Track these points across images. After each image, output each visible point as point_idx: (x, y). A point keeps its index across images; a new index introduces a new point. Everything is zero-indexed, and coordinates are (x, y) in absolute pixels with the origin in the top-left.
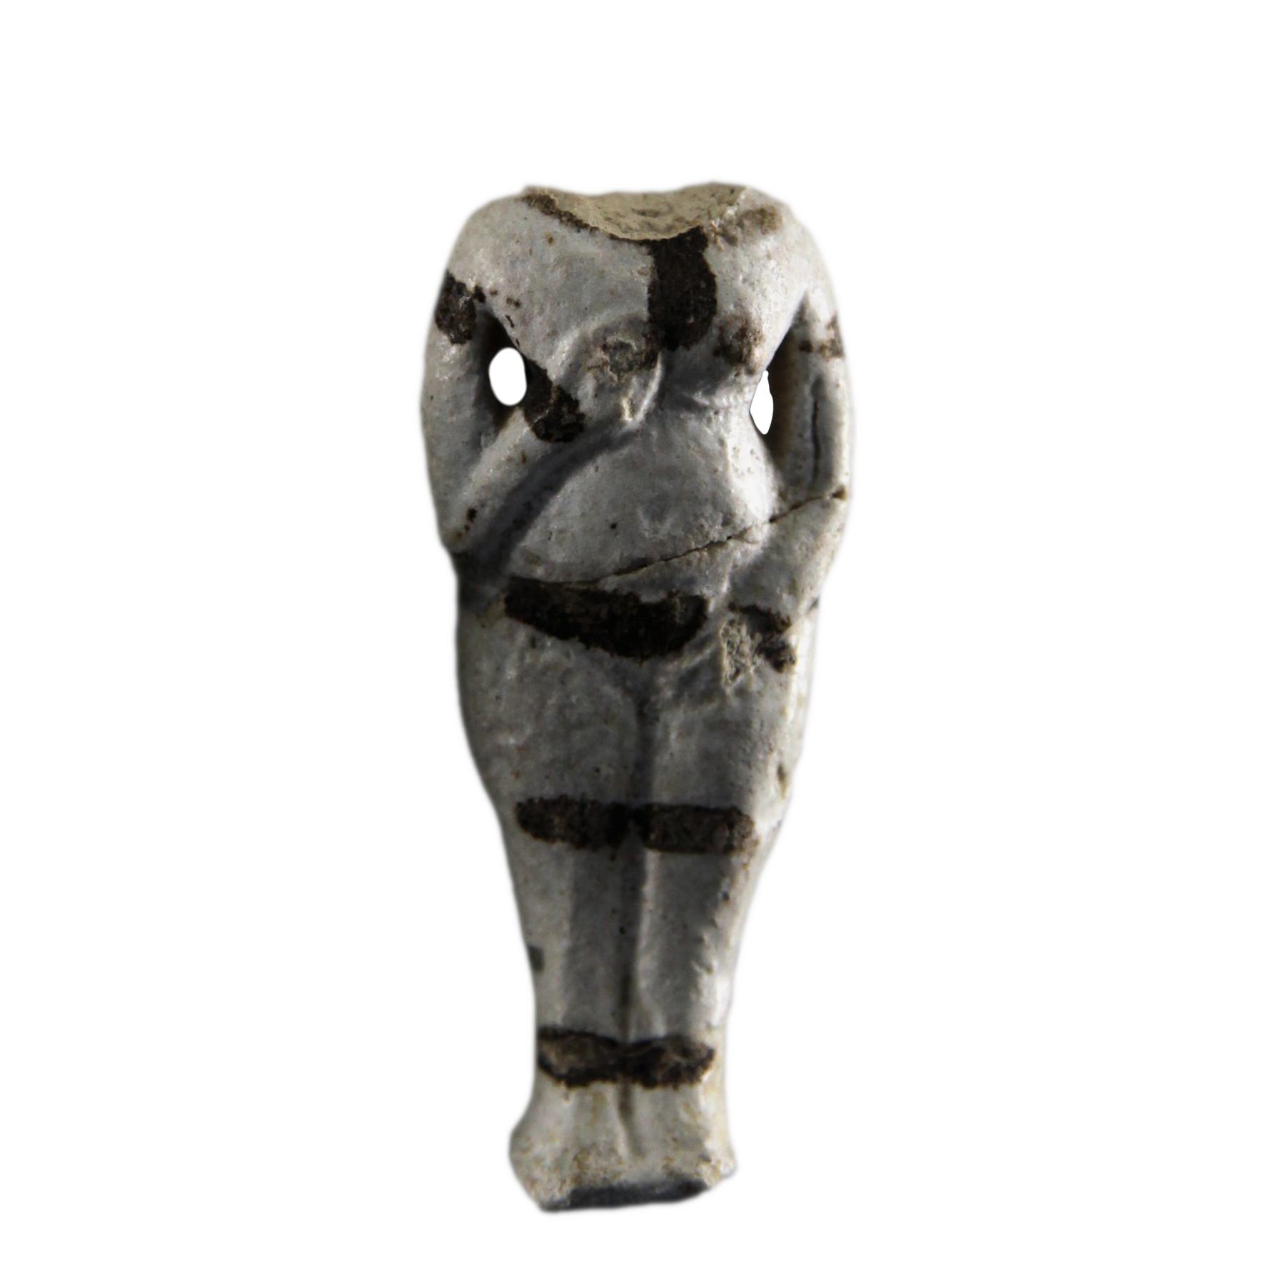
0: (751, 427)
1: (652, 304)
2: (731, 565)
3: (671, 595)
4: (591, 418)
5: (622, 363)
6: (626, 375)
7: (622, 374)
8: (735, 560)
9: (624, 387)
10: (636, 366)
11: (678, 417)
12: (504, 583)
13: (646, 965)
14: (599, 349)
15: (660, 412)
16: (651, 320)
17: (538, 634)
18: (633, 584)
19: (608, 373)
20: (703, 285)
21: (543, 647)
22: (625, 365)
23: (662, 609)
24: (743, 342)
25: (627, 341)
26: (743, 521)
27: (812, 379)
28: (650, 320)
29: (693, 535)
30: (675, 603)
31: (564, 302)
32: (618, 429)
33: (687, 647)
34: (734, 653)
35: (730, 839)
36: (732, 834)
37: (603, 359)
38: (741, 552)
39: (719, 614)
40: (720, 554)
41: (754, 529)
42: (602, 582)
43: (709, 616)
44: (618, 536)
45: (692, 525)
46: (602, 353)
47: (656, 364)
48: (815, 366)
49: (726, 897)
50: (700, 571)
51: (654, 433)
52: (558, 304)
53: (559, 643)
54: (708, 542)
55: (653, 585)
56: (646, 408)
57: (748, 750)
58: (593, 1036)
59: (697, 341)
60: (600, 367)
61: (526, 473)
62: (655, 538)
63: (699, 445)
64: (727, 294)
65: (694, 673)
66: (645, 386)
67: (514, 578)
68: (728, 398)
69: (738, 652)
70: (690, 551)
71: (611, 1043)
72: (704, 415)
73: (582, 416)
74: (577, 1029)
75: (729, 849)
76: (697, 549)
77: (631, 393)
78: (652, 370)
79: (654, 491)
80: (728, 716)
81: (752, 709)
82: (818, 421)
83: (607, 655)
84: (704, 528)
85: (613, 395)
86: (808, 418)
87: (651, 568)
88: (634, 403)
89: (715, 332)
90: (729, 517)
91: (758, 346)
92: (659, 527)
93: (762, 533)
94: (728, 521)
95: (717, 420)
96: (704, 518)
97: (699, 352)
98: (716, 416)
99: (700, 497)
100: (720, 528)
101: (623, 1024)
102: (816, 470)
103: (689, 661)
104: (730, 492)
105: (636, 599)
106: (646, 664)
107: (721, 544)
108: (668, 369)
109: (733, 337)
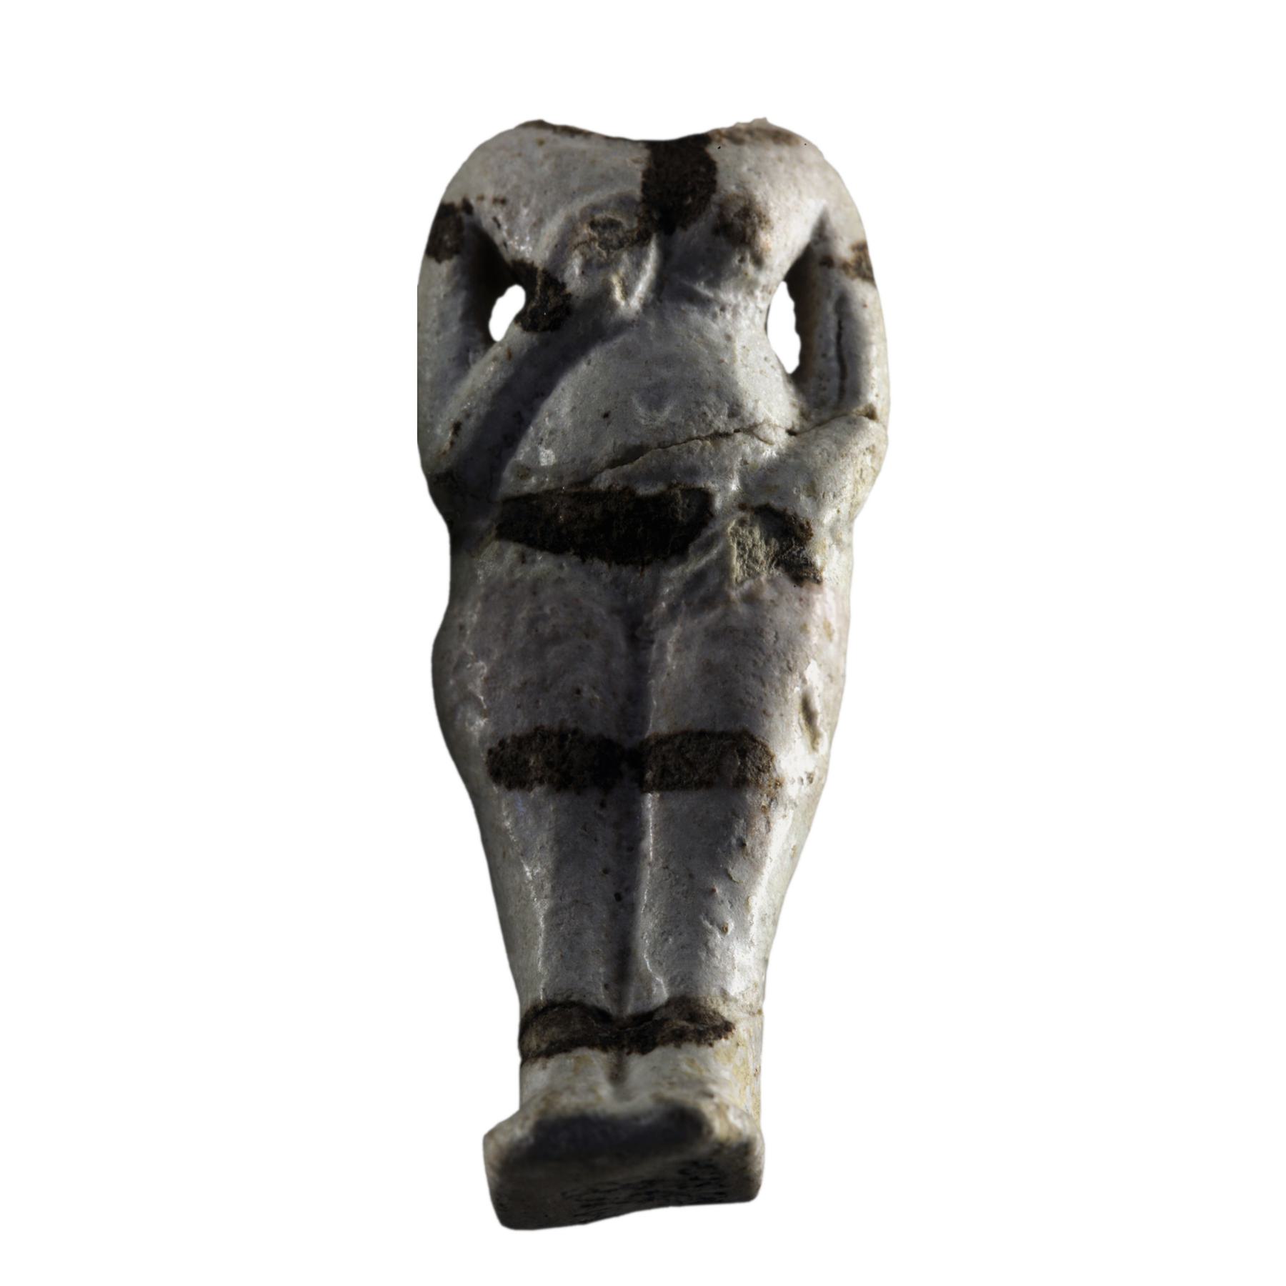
0: (764, 320)
1: (645, 187)
2: (740, 459)
3: (670, 486)
4: (578, 297)
5: (612, 240)
6: (615, 252)
7: (611, 251)
8: (744, 455)
9: (613, 264)
10: (628, 244)
11: (679, 309)
12: (496, 512)
13: (647, 925)
14: (586, 225)
15: (658, 304)
16: (645, 200)
17: (529, 551)
18: (628, 477)
19: (595, 249)
20: (703, 169)
21: (534, 561)
22: (615, 242)
23: (660, 502)
24: (745, 222)
25: (619, 219)
26: (752, 415)
27: (835, 295)
28: (644, 201)
29: (694, 422)
30: (676, 495)
31: (551, 190)
32: (609, 312)
33: (691, 548)
34: (746, 556)
35: (742, 770)
36: (744, 764)
37: (590, 234)
38: (751, 449)
39: (727, 513)
40: (726, 445)
41: (765, 426)
42: (596, 480)
43: (717, 514)
44: (610, 426)
45: (694, 410)
46: (590, 229)
47: (649, 242)
48: (837, 281)
49: (742, 845)
50: (703, 461)
51: (652, 323)
52: (545, 192)
53: (551, 558)
54: (712, 431)
55: (650, 476)
56: (642, 295)
57: (761, 664)
58: (580, 1005)
59: (695, 220)
60: (588, 243)
61: (512, 371)
62: (652, 425)
63: (702, 336)
64: (729, 177)
65: (700, 577)
66: (638, 266)
67: (508, 500)
68: (736, 297)
69: (750, 556)
70: (691, 439)
71: (603, 1016)
72: (708, 309)
73: (569, 296)
74: (559, 999)
75: (741, 783)
76: (699, 438)
77: (622, 271)
78: (644, 248)
79: (650, 379)
80: (733, 622)
81: (764, 617)
82: (843, 340)
83: (605, 565)
84: (707, 416)
85: (602, 271)
86: (832, 336)
87: (648, 455)
88: (627, 284)
89: (714, 209)
90: (735, 407)
91: (764, 230)
92: (657, 415)
93: (780, 439)
94: (735, 410)
95: (724, 317)
96: (706, 405)
97: (694, 234)
98: (722, 313)
99: (702, 384)
100: (726, 418)
101: (620, 1000)
102: (842, 391)
103: (696, 564)
104: (737, 383)
105: (632, 493)
106: (647, 572)
107: (727, 435)
108: (666, 256)
109: (735, 216)
